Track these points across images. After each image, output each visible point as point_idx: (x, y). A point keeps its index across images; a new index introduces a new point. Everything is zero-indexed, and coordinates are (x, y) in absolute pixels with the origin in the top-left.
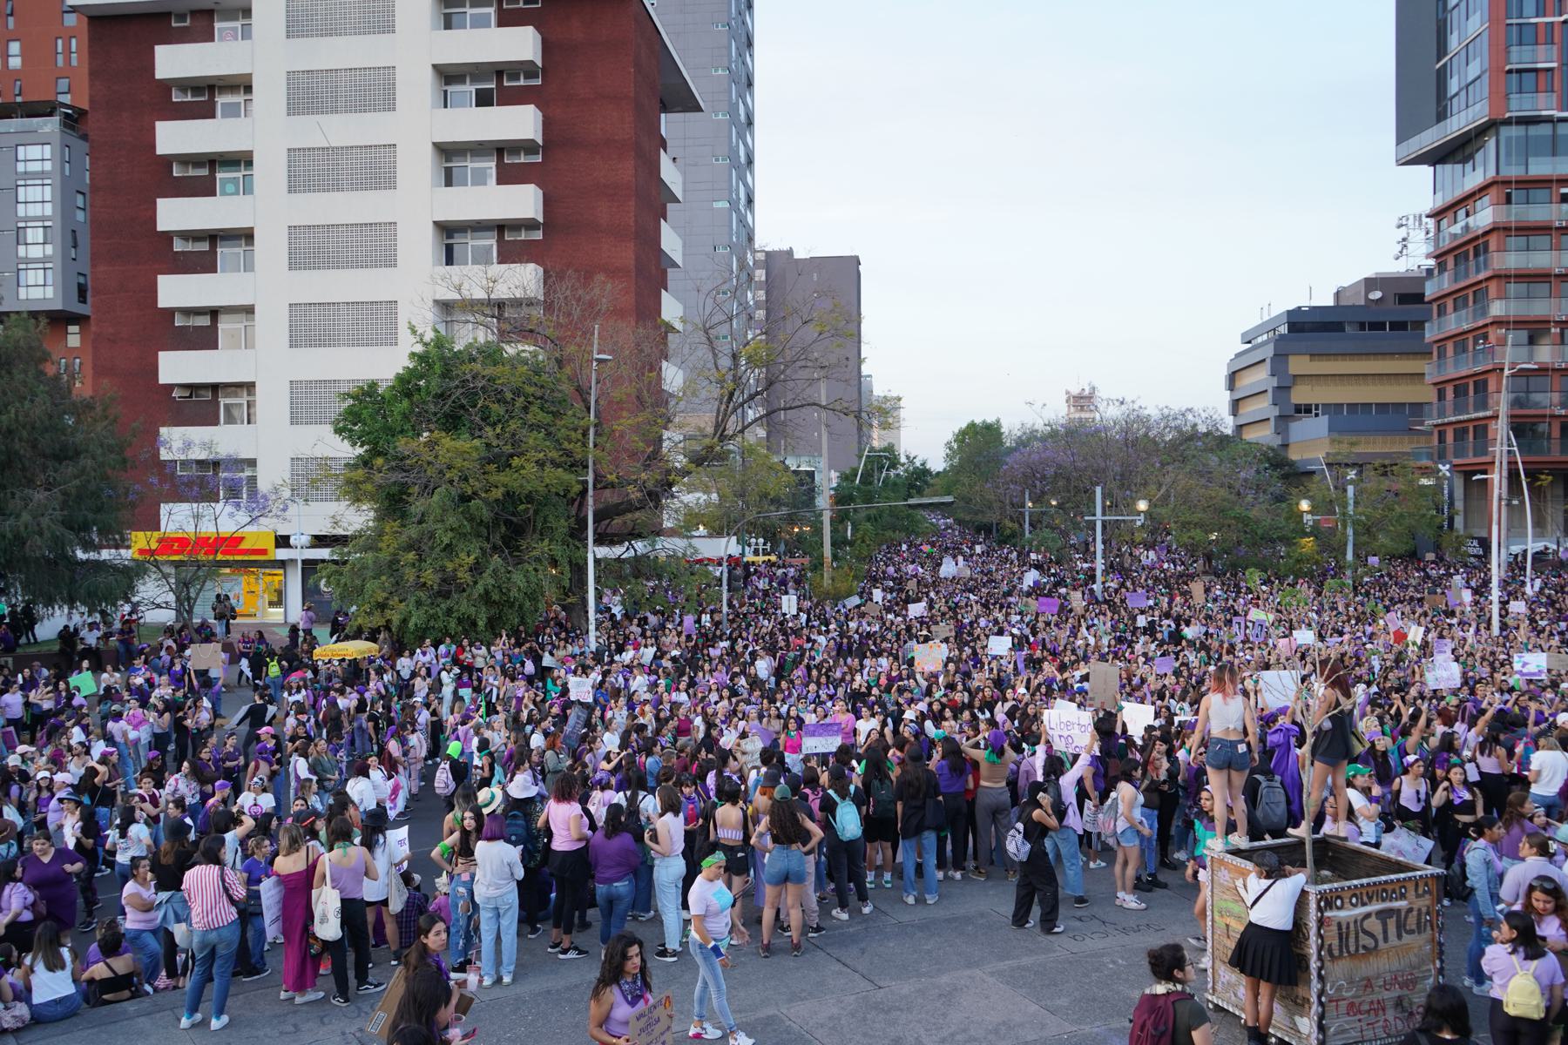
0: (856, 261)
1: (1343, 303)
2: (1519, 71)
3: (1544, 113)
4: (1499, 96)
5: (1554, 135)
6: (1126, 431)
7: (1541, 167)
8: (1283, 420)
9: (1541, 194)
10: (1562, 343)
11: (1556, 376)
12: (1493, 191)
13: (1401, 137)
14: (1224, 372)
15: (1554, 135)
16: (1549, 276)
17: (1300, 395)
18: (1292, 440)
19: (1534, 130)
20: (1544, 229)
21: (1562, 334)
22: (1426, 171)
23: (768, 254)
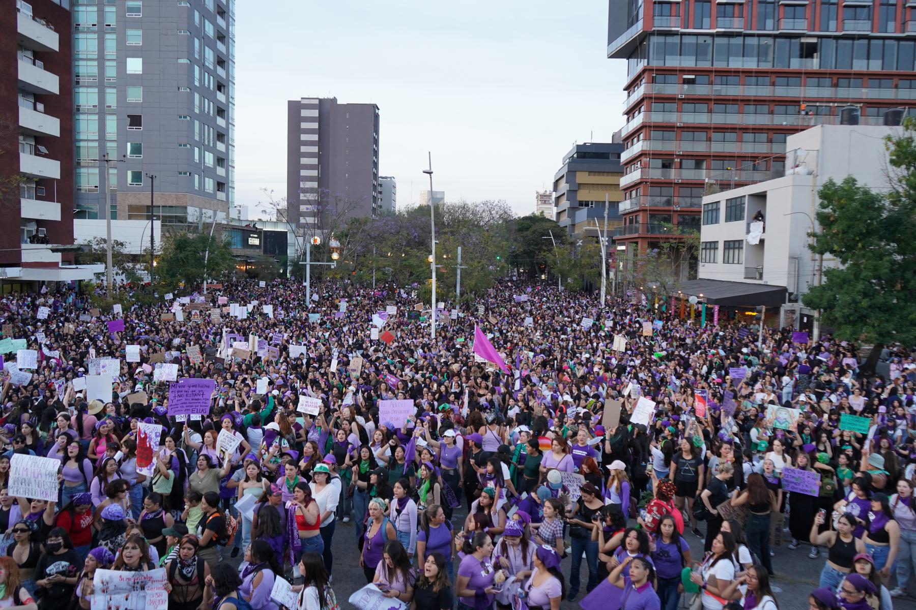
0: (289, 102)
1: (615, 142)
2: (660, 3)
3: (673, 29)
4: (649, 19)
6: (408, 212)
7: (673, 62)
8: (573, 209)
9: (670, 78)
10: (681, 167)
11: (677, 187)
12: (646, 75)
13: (610, 41)
14: (553, 181)
16: (674, 127)
17: (583, 195)
18: (577, 221)
19: (670, 39)
20: (671, 99)
21: (681, 163)
22: (624, 61)
23: (320, 100)
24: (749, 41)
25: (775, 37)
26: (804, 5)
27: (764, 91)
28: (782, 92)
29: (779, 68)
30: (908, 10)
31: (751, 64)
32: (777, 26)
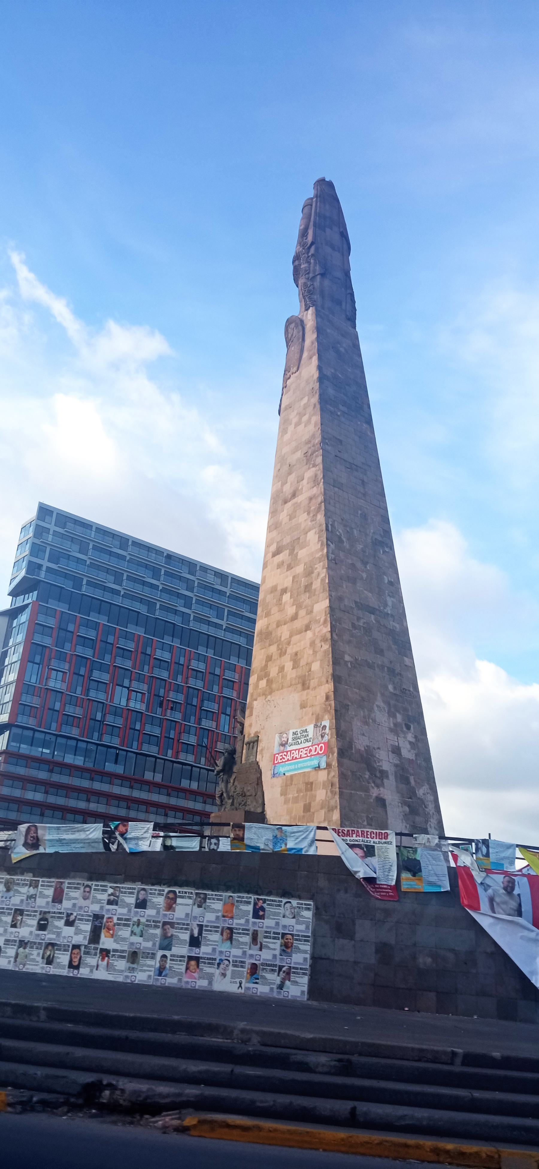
5: (33, 737)
15: (33, 737)
24: (80, 744)
25: (97, 745)
26: (119, 727)
27: (85, 784)
28: (97, 786)
29: (97, 768)
30: (180, 744)
31: (79, 761)
32: (100, 738)
